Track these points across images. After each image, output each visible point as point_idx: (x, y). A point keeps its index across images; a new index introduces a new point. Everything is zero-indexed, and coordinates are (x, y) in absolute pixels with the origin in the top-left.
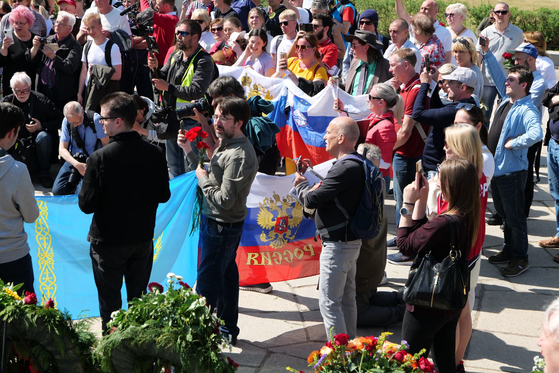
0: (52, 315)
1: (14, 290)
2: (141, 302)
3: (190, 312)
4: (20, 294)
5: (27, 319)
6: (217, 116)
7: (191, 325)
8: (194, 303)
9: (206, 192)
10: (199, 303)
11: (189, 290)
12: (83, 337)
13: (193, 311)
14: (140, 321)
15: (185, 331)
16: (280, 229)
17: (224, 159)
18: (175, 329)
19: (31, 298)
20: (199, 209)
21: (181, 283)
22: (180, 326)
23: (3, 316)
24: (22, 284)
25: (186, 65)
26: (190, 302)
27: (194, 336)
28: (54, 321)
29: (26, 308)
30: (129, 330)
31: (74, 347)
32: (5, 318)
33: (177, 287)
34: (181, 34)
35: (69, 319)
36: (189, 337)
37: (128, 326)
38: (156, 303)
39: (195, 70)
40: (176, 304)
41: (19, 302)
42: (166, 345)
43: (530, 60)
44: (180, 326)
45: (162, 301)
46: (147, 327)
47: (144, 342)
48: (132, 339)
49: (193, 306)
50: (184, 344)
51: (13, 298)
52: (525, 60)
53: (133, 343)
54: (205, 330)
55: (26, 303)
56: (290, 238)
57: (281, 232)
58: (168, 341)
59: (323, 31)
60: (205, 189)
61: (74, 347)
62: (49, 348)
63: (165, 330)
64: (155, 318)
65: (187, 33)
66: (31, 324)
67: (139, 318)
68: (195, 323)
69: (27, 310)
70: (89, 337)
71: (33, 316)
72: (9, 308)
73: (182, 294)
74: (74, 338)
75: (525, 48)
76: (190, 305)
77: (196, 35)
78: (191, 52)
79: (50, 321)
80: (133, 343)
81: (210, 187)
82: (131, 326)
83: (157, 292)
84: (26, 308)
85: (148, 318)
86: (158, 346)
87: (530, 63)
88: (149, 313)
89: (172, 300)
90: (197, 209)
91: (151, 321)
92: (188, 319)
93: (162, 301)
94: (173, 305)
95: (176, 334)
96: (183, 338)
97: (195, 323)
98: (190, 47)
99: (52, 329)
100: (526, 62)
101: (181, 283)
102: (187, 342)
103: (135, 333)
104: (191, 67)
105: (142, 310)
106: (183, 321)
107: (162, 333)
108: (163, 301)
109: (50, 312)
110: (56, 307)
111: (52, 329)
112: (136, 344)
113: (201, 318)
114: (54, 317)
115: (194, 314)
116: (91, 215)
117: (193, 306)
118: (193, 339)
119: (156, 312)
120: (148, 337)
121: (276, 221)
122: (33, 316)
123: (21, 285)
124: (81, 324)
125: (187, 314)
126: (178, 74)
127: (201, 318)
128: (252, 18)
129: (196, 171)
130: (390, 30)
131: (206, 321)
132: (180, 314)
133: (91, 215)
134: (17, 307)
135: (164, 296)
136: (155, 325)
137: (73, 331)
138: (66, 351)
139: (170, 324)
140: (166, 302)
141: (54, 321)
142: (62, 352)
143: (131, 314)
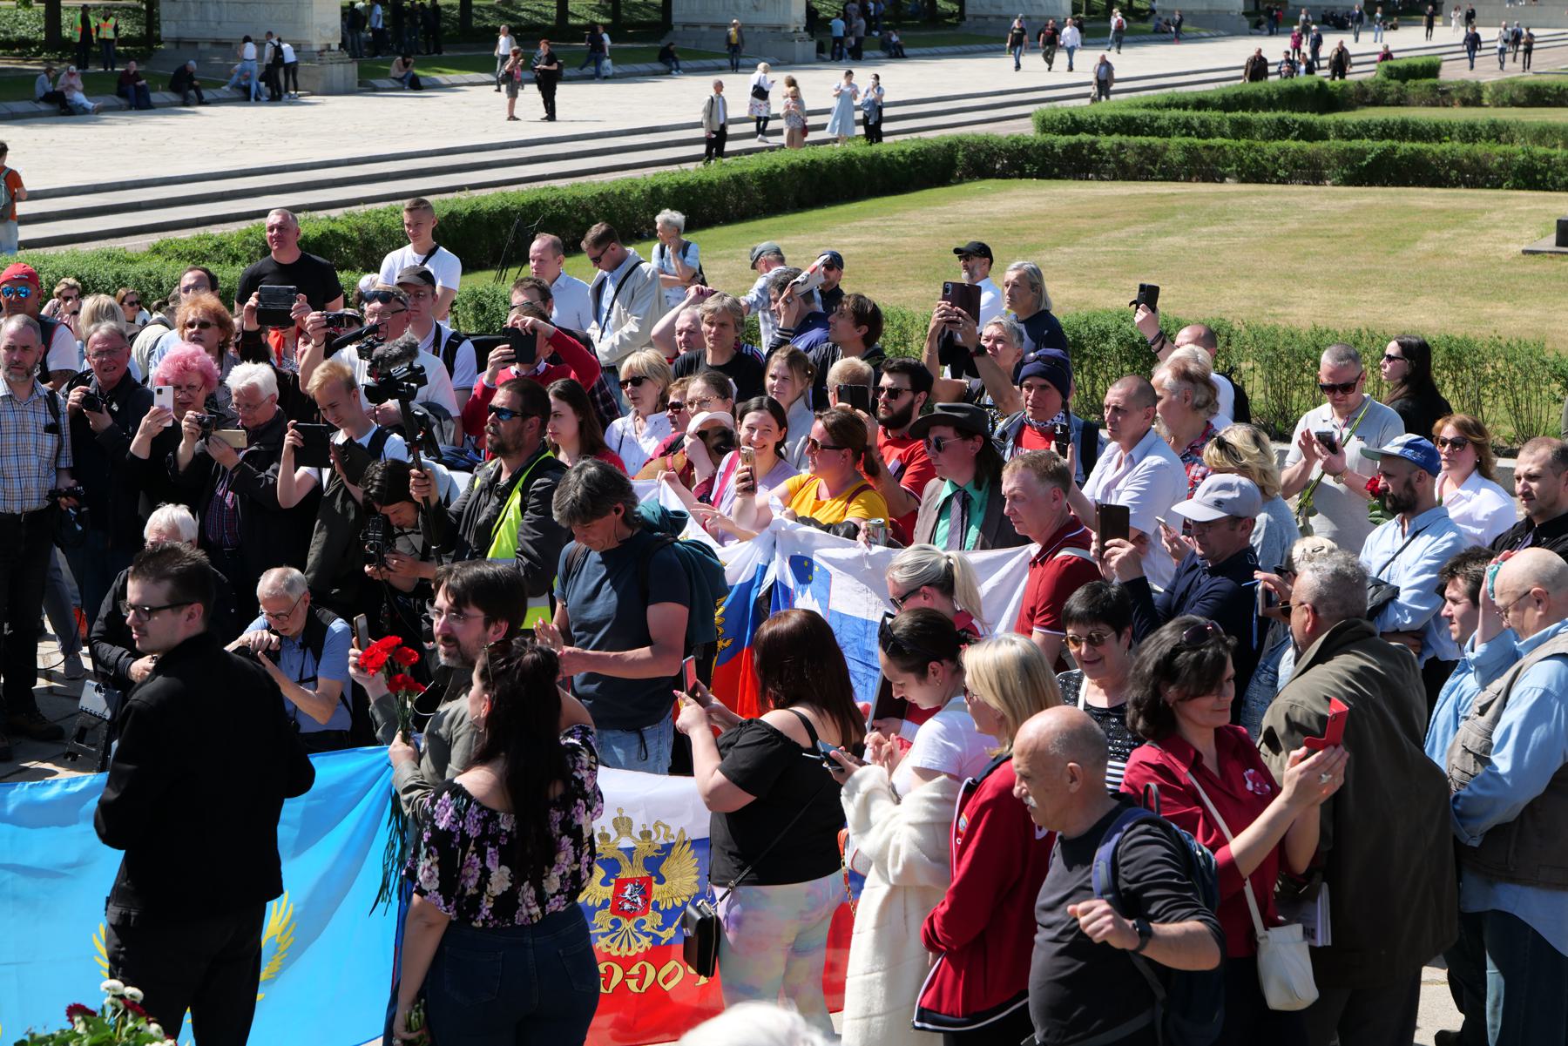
6: (440, 612)
9: (408, 802)
16: (627, 906)
17: (452, 720)
20: (398, 847)
25: (505, 494)
34: (498, 415)
39: (523, 507)
43: (1420, 479)
52: (1406, 476)
56: (661, 934)
57: (629, 915)
59: (912, 404)
60: (406, 797)
65: (512, 413)
75: (1408, 445)
77: (535, 420)
78: (518, 461)
81: (419, 792)
87: (1418, 487)
90: (394, 846)
98: (518, 448)
100: (1408, 484)
104: (515, 499)
116: (122, 852)
121: (612, 888)
126: (482, 518)
128: (774, 377)
129: (391, 747)
130: (1106, 402)
133: (122, 852)
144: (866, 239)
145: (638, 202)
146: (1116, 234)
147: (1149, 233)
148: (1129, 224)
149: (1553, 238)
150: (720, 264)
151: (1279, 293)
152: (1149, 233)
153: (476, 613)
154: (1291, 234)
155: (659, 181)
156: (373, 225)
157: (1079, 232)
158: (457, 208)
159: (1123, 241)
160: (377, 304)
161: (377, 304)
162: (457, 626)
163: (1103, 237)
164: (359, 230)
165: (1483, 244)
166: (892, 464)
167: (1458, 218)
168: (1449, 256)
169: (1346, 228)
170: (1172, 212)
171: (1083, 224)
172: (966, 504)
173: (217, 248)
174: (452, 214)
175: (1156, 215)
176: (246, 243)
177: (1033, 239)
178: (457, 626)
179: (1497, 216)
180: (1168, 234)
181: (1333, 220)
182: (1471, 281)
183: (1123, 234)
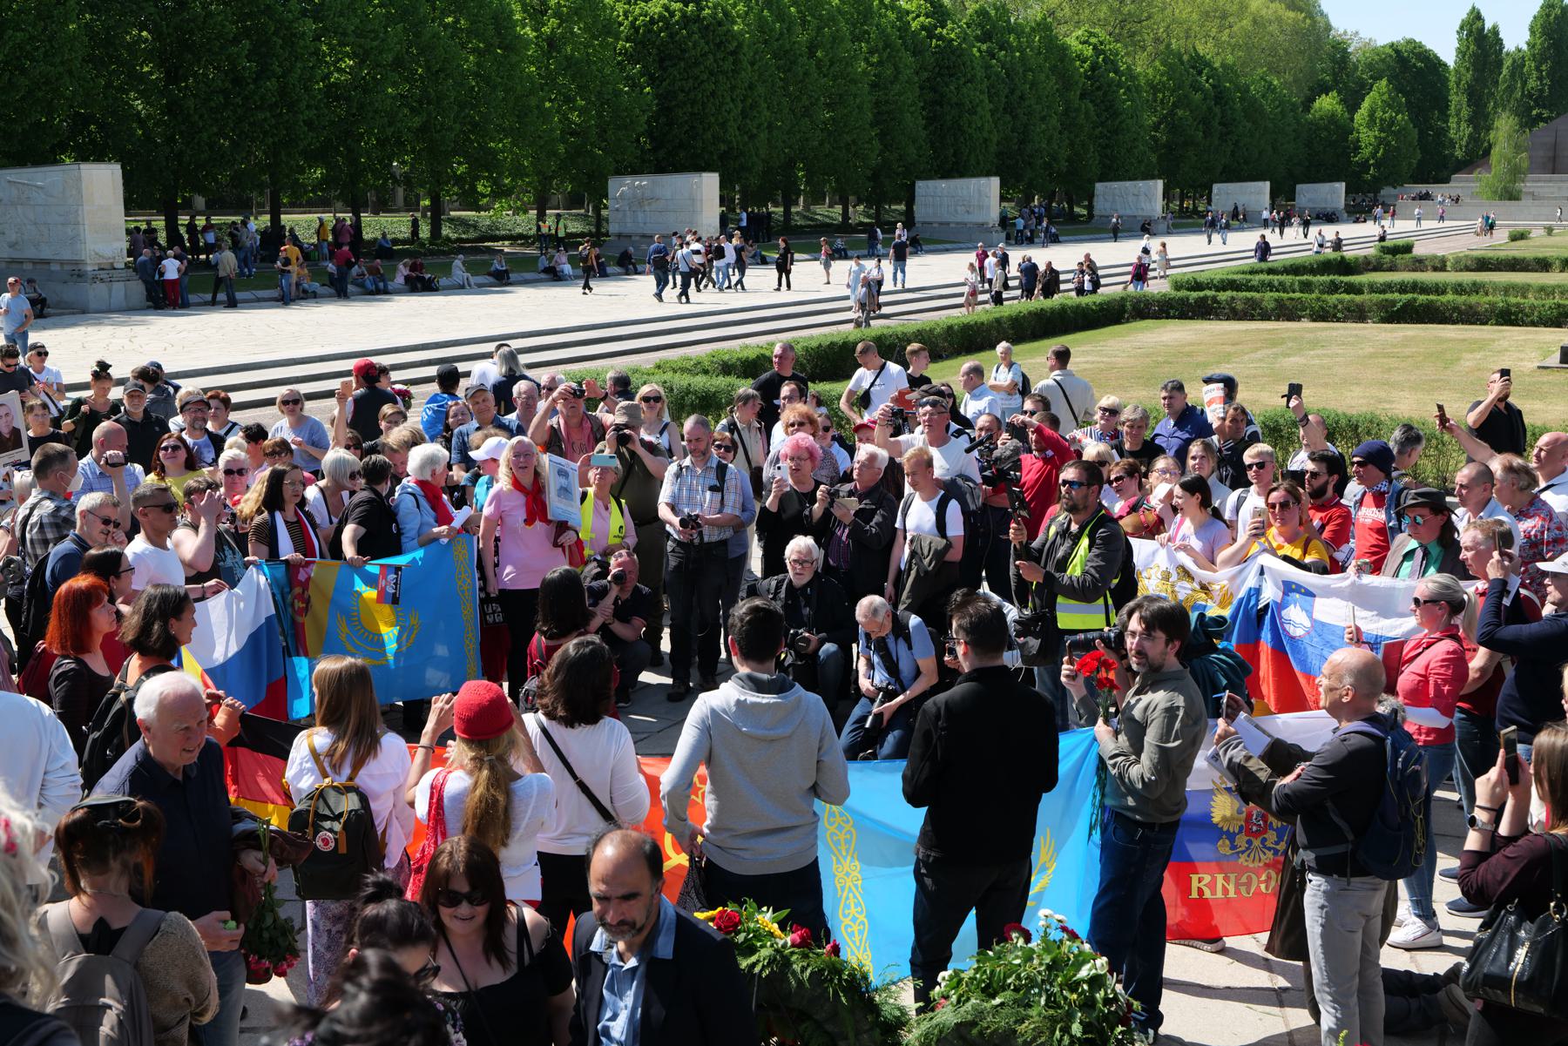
0: (836, 970)
1: (773, 920)
2: (991, 959)
3: (1078, 983)
4: (782, 927)
5: (794, 973)
6: (1133, 634)
7: (1082, 1007)
8: (1088, 966)
10: (1095, 967)
11: (1078, 943)
12: (888, 1011)
13: (1084, 981)
14: (989, 991)
15: (1070, 1017)
18: (1051, 1012)
19: (801, 937)
21: (1064, 929)
22: (1060, 1007)
23: (754, 965)
24: (785, 912)
26: (1079, 965)
27: (1087, 1027)
28: (840, 979)
29: (792, 953)
30: (968, 1006)
31: (872, 1029)
32: (757, 970)
33: (1056, 935)
35: (865, 977)
36: (1076, 1029)
37: (968, 999)
38: (1018, 961)
40: (1054, 967)
41: (781, 943)
42: (1034, 1039)
44: (1060, 1007)
45: (1028, 958)
46: (1002, 1004)
47: (996, 1030)
48: (973, 1024)
49: (1084, 972)
50: (1066, 1040)
51: (771, 934)
53: (975, 1031)
54: (1106, 1017)
55: (793, 945)
58: (1038, 1032)
59: (1327, 483)
61: (872, 1029)
62: (829, 1027)
63: (1033, 1012)
64: (1016, 990)
65: (1080, 484)
66: (800, 983)
67: (988, 986)
68: (1088, 1004)
69: (794, 958)
70: (898, 1013)
71: (804, 969)
72: (765, 952)
73: (1064, 949)
74: (872, 1012)
76: (1079, 970)
77: (1095, 487)
78: (1083, 517)
79: (831, 980)
80: (975, 1031)
82: (973, 1001)
83: (1021, 942)
84: (792, 953)
85: (1004, 988)
86: (1020, 1040)
88: (1006, 978)
89: (1047, 960)
91: (1008, 993)
92: (1075, 996)
93: (1028, 958)
94: (1049, 968)
95: (1053, 1020)
96: (1066, 1030)
97: (1088, 1004)
99: (836, 994)
101: (1064, 929)
102: (1072, 1037)
103: (980, 1013)
104: (1085, 542)
105: (992, 972)
106: (1065, 998)
107: (1028, 1017)
108: (1031, 959)
109: (833, 964)
110: (843, 955)
111: (836, 994)
112: (981, 1033)
113: (1100, 995)
114: (840, 972)
115: (1086, 987)
117: (1084, 972)
118: (1084, 1032)
119: (1019, 978)
120: (1001, 1022)
122: (804, 969)
123: (785, 912)
124: (886, 988)
125: (1074, 986)
126: (1060, 554)
127: (1100, 995)
128: (1194, 458)
131: (1107, 1002)
132: (1060, 985)
134: (777, 951)
135: (1032, 951)
136: (1015, 1001)
137: (871, 999)
138: (858, 1034)
139: (1043, 1002)
140: (1036, 962)
141: (840, 979)
142: (851, 1035)
143: (972, 979)
144: (1090, 358)
145: (940, 335)
147: (1276, 356)
148: (1257, 349)
149: (1558, 355)
151: (1383, 394)
152: (1276, 356)
153: (1160, 636)
154: (1372, 356)
155: (951, 322)
157: (1229, 354)
158: (835, 339)
159: (1261, 360)
160: (928, 408)
161: (928, 408)
162: (1147, 644)
163: (1246, 358)
166: (1316, 523)
167: (1481, 345)
169: (1407, 351)
170: (1283, 342)
172: (1426, 554)
175: (1274, 344)
178: (1147, 644)
179: (1505, 344)
180: (1289, 355)
181: (1395, 346)
183: (1259, 354)
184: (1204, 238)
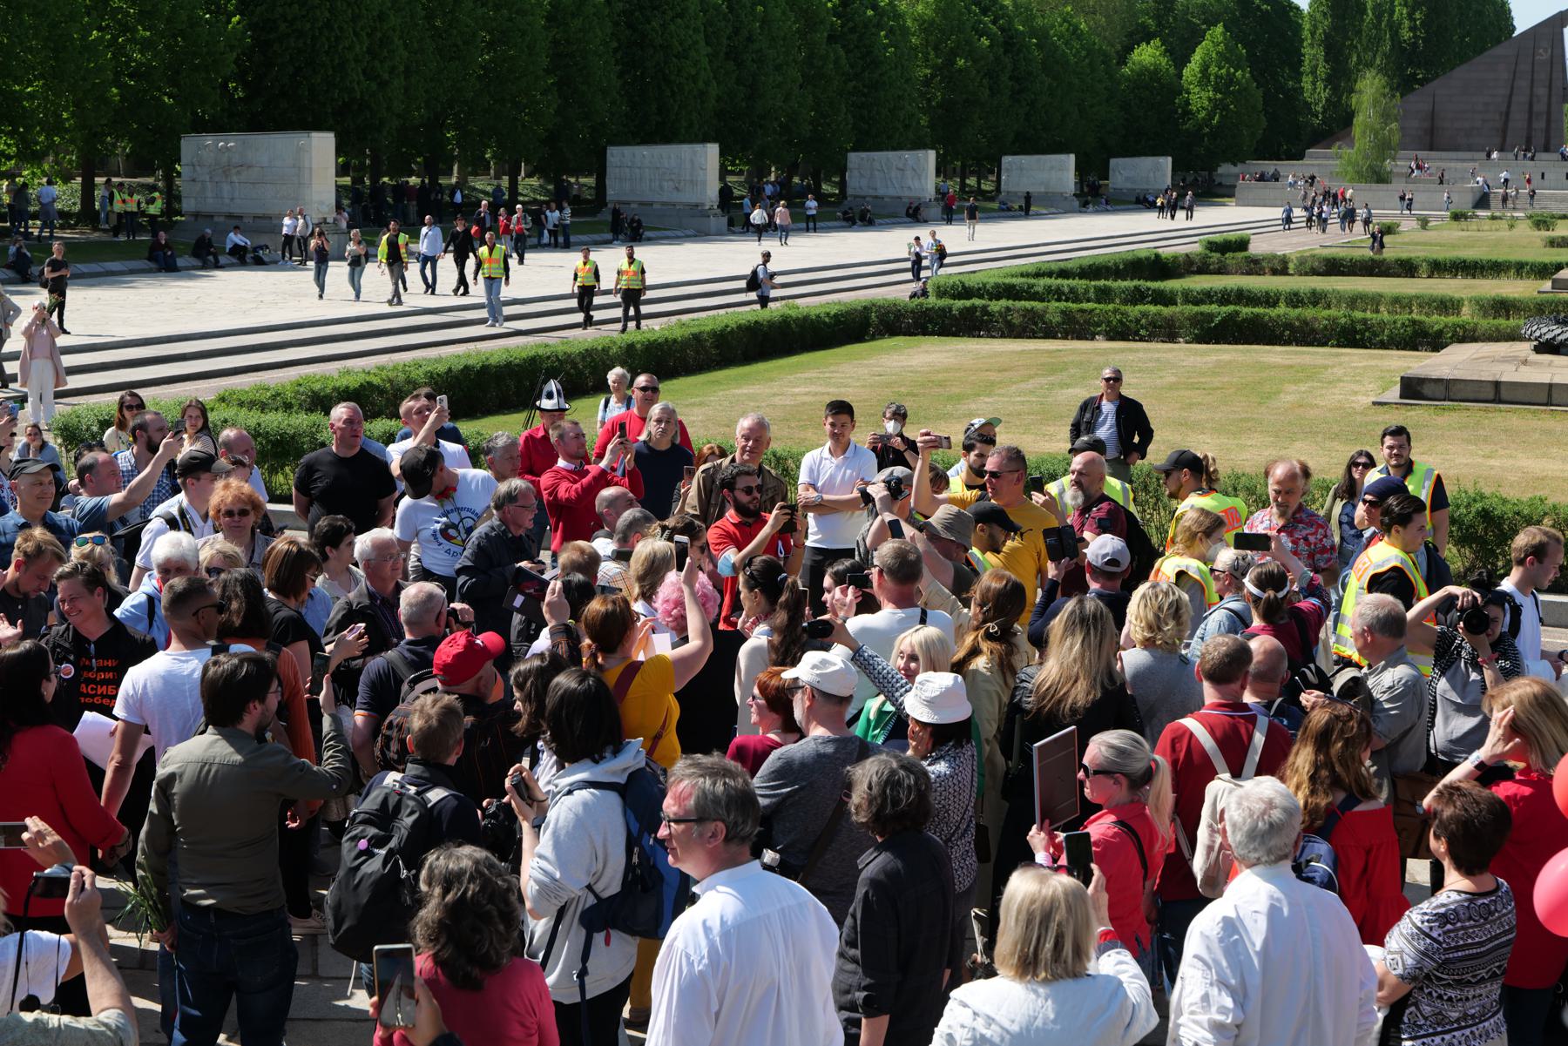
144: (813, 389)
146: (1023, 385)
148: (1031, 377)
149: (1398, 387)
150: (696, 410)
154: (1172, 387)
156: (402, 377)
157: (993, 384)
158: (471, 362)
159: (1031, 392)
163: (1014, 388)
164: (390, 381)
165: (1334, 396)
167: (1309, 374)
168: (1313, 406)
169: (1217, 381)
171: (994, 376)
173: (274, 397)
174: (466, 367)
175: (1053, 370)
176: (297, 392)
177: (955, 390)
179: (1339, 371)
180: (1068, 386)
181: (1203, 374)
182: (1336, 428)
183: (1030, 385)
184: (307, 276)
